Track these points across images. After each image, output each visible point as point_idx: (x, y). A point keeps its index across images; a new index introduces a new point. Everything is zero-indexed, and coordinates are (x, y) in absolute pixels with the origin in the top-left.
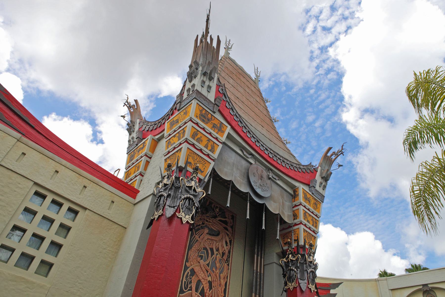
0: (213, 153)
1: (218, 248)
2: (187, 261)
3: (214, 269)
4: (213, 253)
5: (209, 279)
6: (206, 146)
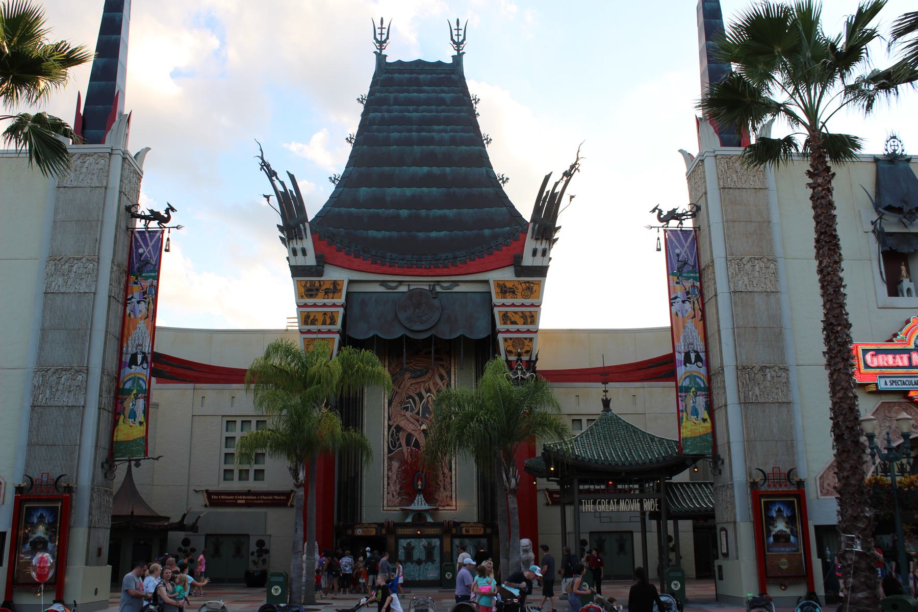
0: (334, 324)
1: (429, 388)
2: (389, 419)
3: (427, 415)
5: (424, 427)
6: (324, 323)
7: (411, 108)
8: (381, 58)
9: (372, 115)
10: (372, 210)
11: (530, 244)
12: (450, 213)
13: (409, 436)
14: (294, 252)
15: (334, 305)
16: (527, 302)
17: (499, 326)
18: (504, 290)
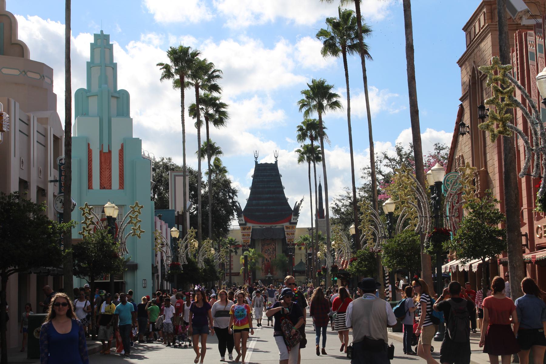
4: (269, 250)
6: (247, 236)
7: (265, 177)
8: (256, 162)
9: (255, 180)
10: (256, 207)
11: (293, 217)
12: (275, 207)
13: (267, 259)
14: (240, 220)
15: (249, 232)
16: (292, 230)
17: (286, 236)
18: (287, 228)
